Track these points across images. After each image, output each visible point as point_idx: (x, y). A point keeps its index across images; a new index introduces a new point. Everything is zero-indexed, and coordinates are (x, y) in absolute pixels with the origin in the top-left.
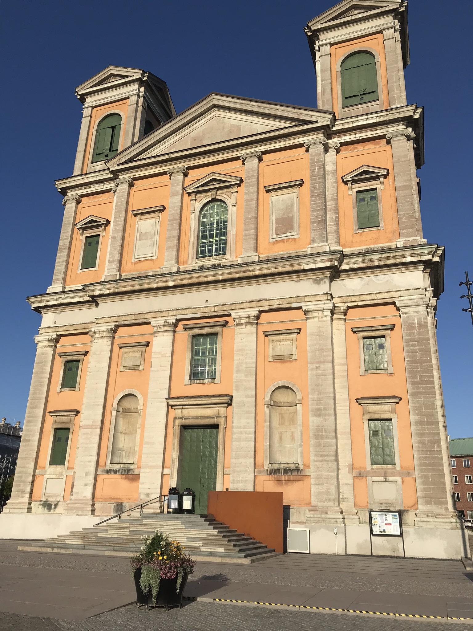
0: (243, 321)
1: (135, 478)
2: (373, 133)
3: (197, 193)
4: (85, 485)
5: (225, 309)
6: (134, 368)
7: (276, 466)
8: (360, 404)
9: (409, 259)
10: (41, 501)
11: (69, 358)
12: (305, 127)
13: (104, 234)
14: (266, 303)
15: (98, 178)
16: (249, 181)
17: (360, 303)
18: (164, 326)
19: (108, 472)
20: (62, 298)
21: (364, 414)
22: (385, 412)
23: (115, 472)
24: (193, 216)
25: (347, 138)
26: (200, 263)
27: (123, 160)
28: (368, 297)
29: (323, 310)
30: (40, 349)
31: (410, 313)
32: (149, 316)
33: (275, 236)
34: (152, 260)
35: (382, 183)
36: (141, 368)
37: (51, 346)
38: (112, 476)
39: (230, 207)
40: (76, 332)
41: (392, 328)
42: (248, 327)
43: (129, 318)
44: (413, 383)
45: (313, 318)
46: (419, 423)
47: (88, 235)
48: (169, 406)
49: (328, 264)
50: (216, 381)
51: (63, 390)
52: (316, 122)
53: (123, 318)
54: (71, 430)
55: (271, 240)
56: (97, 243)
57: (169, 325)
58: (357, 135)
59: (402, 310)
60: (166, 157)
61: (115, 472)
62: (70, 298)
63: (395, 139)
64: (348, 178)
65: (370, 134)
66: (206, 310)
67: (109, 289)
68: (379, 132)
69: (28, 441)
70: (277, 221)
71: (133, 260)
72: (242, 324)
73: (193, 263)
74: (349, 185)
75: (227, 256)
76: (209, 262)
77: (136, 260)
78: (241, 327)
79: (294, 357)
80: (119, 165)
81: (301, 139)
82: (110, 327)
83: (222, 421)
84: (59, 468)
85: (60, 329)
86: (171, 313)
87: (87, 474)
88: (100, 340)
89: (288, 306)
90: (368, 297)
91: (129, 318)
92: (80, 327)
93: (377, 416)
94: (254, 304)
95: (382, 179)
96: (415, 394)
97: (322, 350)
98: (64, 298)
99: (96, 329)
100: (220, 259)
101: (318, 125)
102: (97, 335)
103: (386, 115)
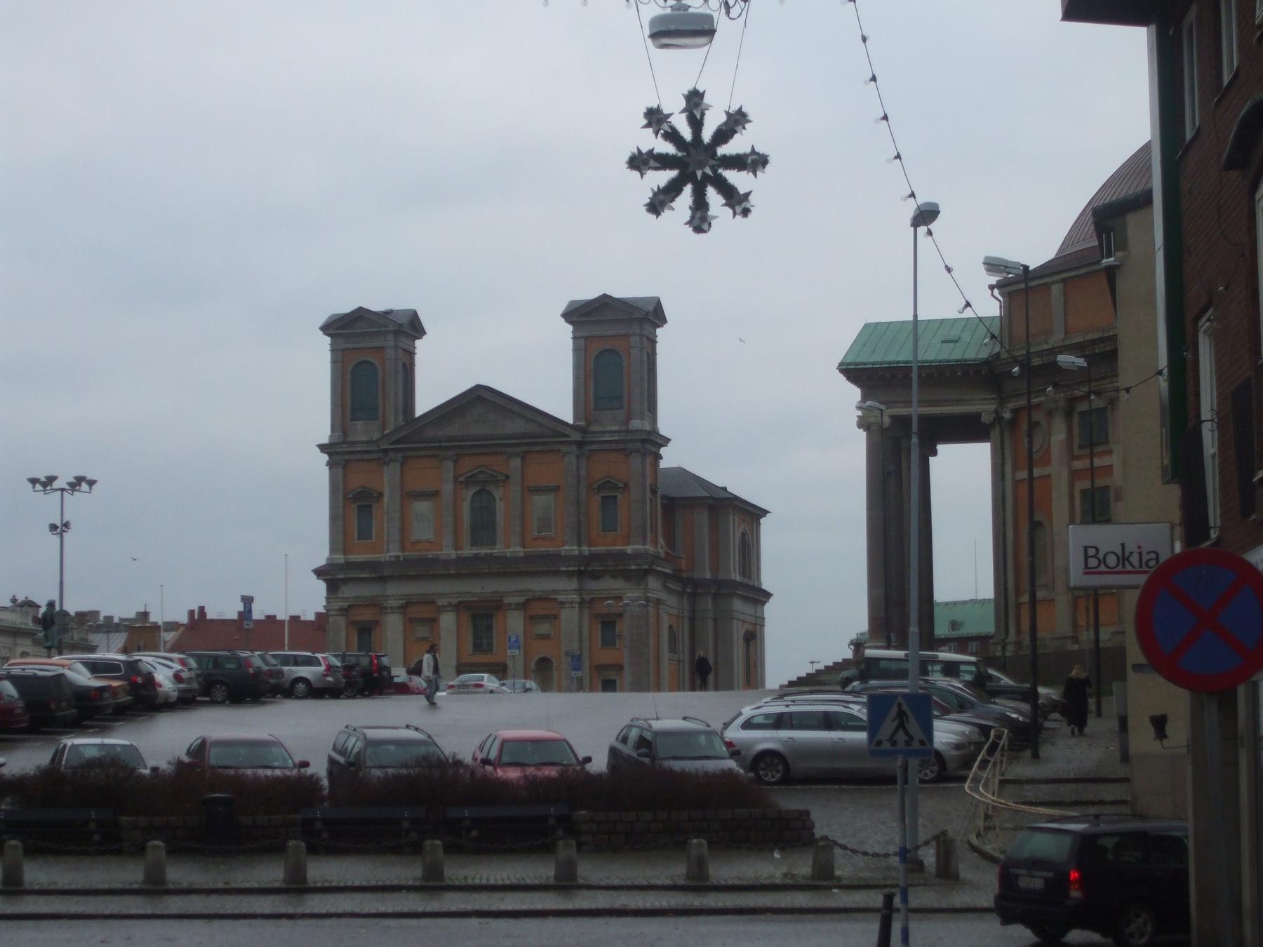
9: (633, 567)
13: (376, 505)
24: (464, 503)
25: (595, 447)
33: (536, 534)
34: (430, 542)
36: (431, 639)
39: (498, 500)
42: (516, 612)
47: (358, 504)
49: (576, 568)
50: (493, 652)
56: (371, 512)
65: (614, 446)
68: (620, 446)
73: (468, 551)
74: (596, 491)
75: (496, 547)
76: (484, 551)
79: (552, 636)
80: (390, 444)
81: (558, 447)
82: (400, 605)
99: (388, 605)
100: (492, 549)
101: (570, 439)
102: (389, 610)
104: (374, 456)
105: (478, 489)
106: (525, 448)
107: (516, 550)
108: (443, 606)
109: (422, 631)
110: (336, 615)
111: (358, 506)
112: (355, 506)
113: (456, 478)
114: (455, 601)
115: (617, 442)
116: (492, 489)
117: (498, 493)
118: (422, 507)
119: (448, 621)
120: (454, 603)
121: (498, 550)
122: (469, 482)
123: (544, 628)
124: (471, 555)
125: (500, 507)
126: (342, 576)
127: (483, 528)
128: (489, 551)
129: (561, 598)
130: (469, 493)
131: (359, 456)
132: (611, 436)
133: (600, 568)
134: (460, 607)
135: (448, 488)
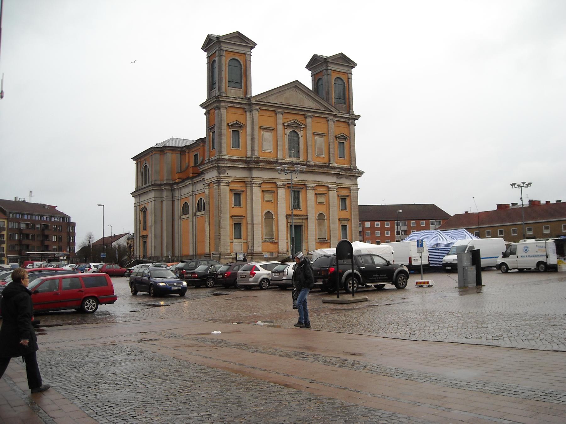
0: (310, 188)
1: (277, 243)
2: (345, 120)
4: (258, 246)
5: (304, 182)
6: (269, 201)
7: (320, 240)
8: (340, 220)
10: (234, 253)
11: (236, 192)
12: (330, 113)
14: (317, 182)
15: (241, 102)
16: (309, 128)
17: (341, 187)
18: (282, 185)
20: (234, 164)
21: (340, 223)
22: (345, 223)
23: (268, 241)
27: (257, 99)
28: (343, 185)
29: (334, 188)
30: (222, 186)
31: (354, 192)
32: (275, 180)
35: (346, 141)
37: (228, 186)
40: (239, 180)
41: (348, 196)
43: (267, 179)
44: (354, 215)
45: (331, 190)
46: (355, 227)
47: (233, 129)
48: (287, 218)
49: (338, 173)
51: (235, 206)
52: (334, 112)
53: (265, 179)
54: (242, 224)
55: (316, 156)
57: (284, 185)
58: (341, 119)
59: (352, 191)
60: (278, 105)
61: (268, 241)
62: (238, 165)
63: (352, 125)
64: (338, 136)
65: (344, 120)
66: (297, 181)
67: (261, 166)
69: (225, 228)
71: (262, 151)
72: (310, 189)
76: (295, 160)
77: (263, 151)
78: (309, 190)
80: (256, 101)
81: (326, 116)
83: (304, 224)
84: (239, 240)
85: (231, 178)
86: (284, 180)
87: (259, 242)
88: (256, 187)
89: (324, 185)
90: (343, 185)
91: (267, 179)
92: (240, 178)
93: (344, 224)
94: (313, 182)
95: (347, 140)
96: (354, 218)
97: (334, 202)
98: (236, 164)
99: (255, 183)
101: (334, 113)
102: (254, 185)
103: (352, 116)
104: (242, 106)
105: (292, 130)
106: (313, 114)
108: (280, 185)
109: (269, 197)
110: (225, 186)
111: (232, 130)
112: (231, 130)
113: (283, 124)
114: (285, 183)
117: (301, 133)
118: (267, 135)
119: (282, 193)
120: (285, 184)
122: (289, 126)
123: (322, 199)
124: (290, 162)
125: (301, 140)
126: (230, 165)
129: (330, 186)
130: (288, 131)
131: (235, 105)
132: (346, 115)
133: (345, 174)
134: (288, 187)
135: (280, 127)
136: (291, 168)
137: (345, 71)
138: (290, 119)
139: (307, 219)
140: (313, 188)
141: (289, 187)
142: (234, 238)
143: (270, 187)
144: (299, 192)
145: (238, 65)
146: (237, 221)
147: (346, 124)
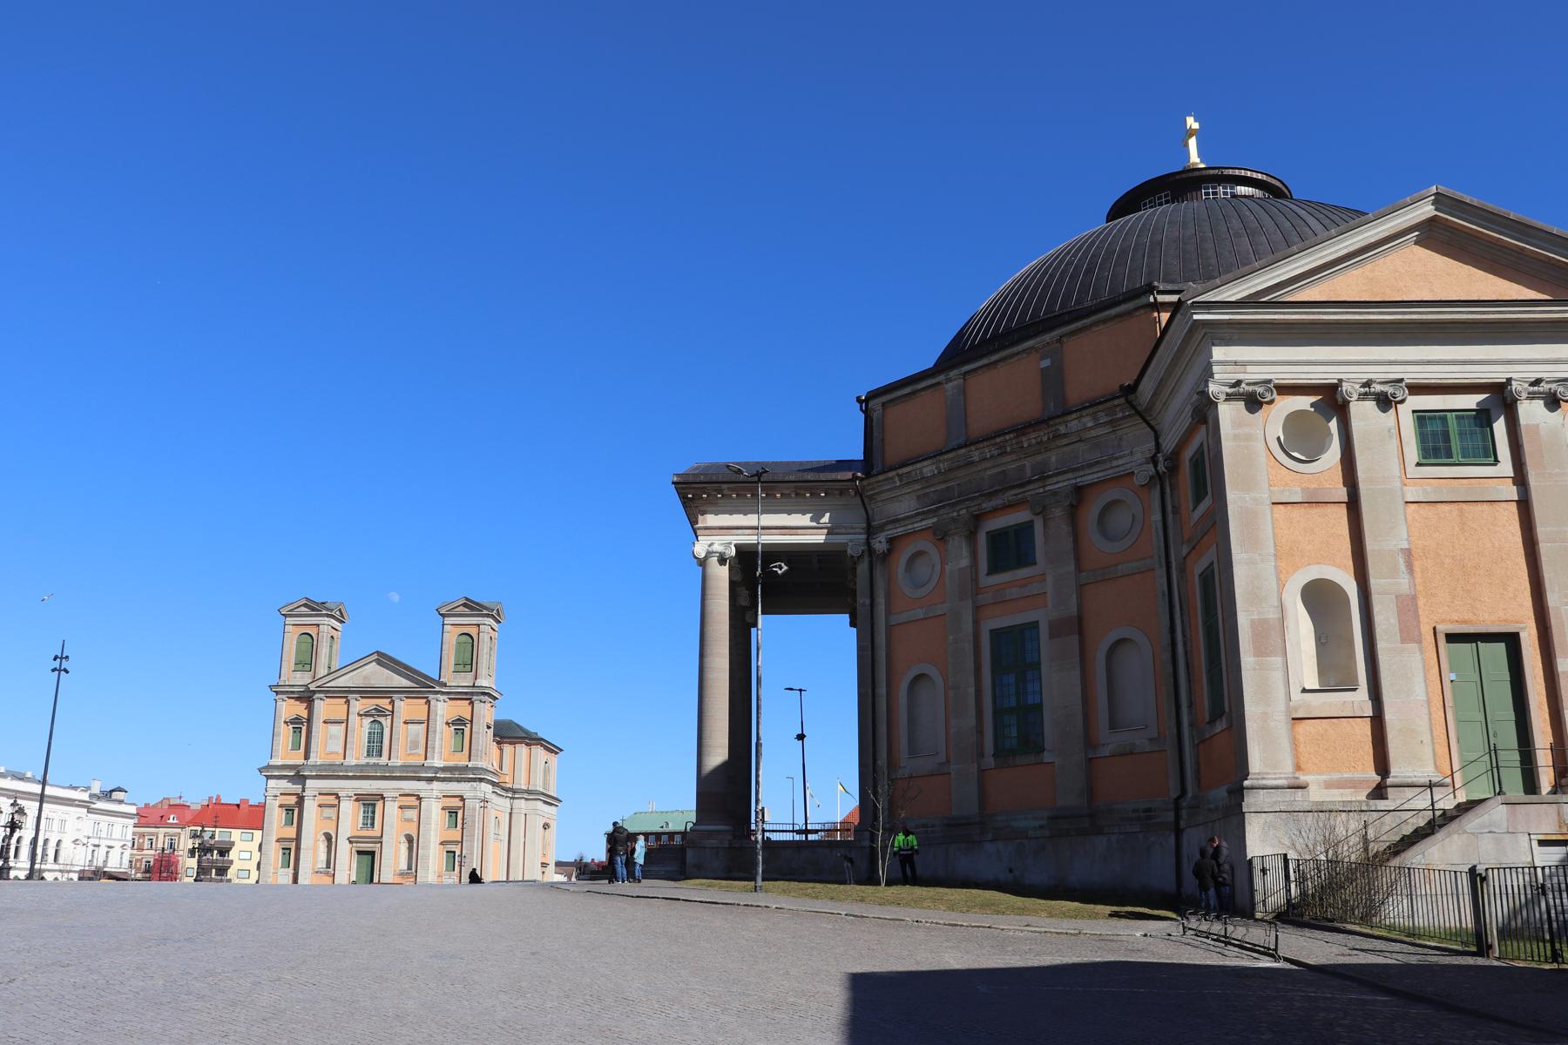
3: (366, 715)
6: (329, 818)
9: (471, 776)
19: (317, 872)
23: (321, 872)
26: (367, 760)
27: (319, 684)
38: (319, 874)
41: (459, 808)
48: (350, 842)
52: (434, 688)
61: (321, 872)
70: (411, 741)
73: (363, 761)
76: (373, 761)
84: (286, 869)
93: (449, 850)
107: (397, 761)
115: (466, 693)
116: (382, 719)
117: (386, 722)
121: (384, 760)
122: (367, 714)
127: (375, 745)
128: (376, 762)
136: (362, 774)
137: (475, 622)
138: (369, 704)
139: (381, 843)
140: (394, 799)
141: (357, 800)
142: (280, 866)
143: (332, 800)
144: (374, 805)
145: (310, 640)
146: (287, 845)
147: (468, 702)
